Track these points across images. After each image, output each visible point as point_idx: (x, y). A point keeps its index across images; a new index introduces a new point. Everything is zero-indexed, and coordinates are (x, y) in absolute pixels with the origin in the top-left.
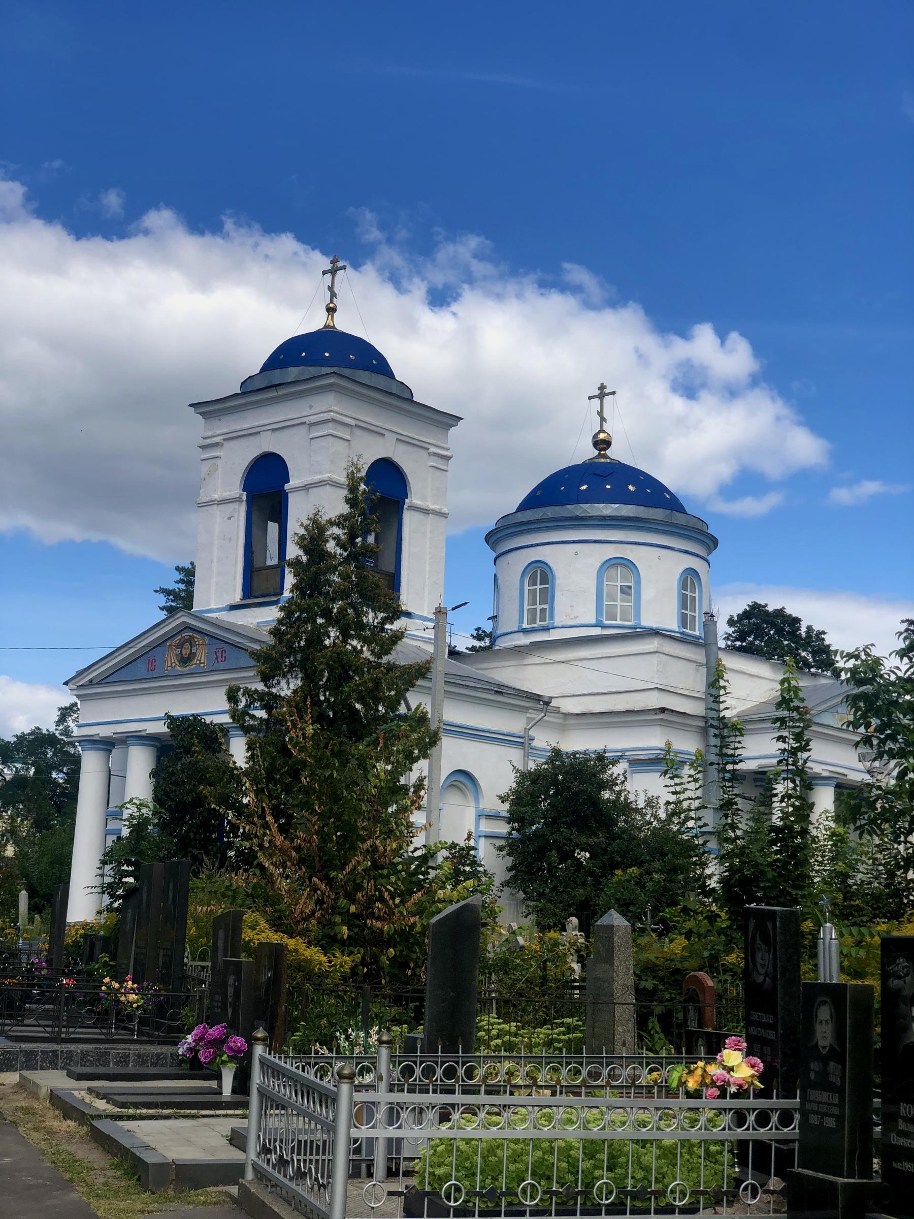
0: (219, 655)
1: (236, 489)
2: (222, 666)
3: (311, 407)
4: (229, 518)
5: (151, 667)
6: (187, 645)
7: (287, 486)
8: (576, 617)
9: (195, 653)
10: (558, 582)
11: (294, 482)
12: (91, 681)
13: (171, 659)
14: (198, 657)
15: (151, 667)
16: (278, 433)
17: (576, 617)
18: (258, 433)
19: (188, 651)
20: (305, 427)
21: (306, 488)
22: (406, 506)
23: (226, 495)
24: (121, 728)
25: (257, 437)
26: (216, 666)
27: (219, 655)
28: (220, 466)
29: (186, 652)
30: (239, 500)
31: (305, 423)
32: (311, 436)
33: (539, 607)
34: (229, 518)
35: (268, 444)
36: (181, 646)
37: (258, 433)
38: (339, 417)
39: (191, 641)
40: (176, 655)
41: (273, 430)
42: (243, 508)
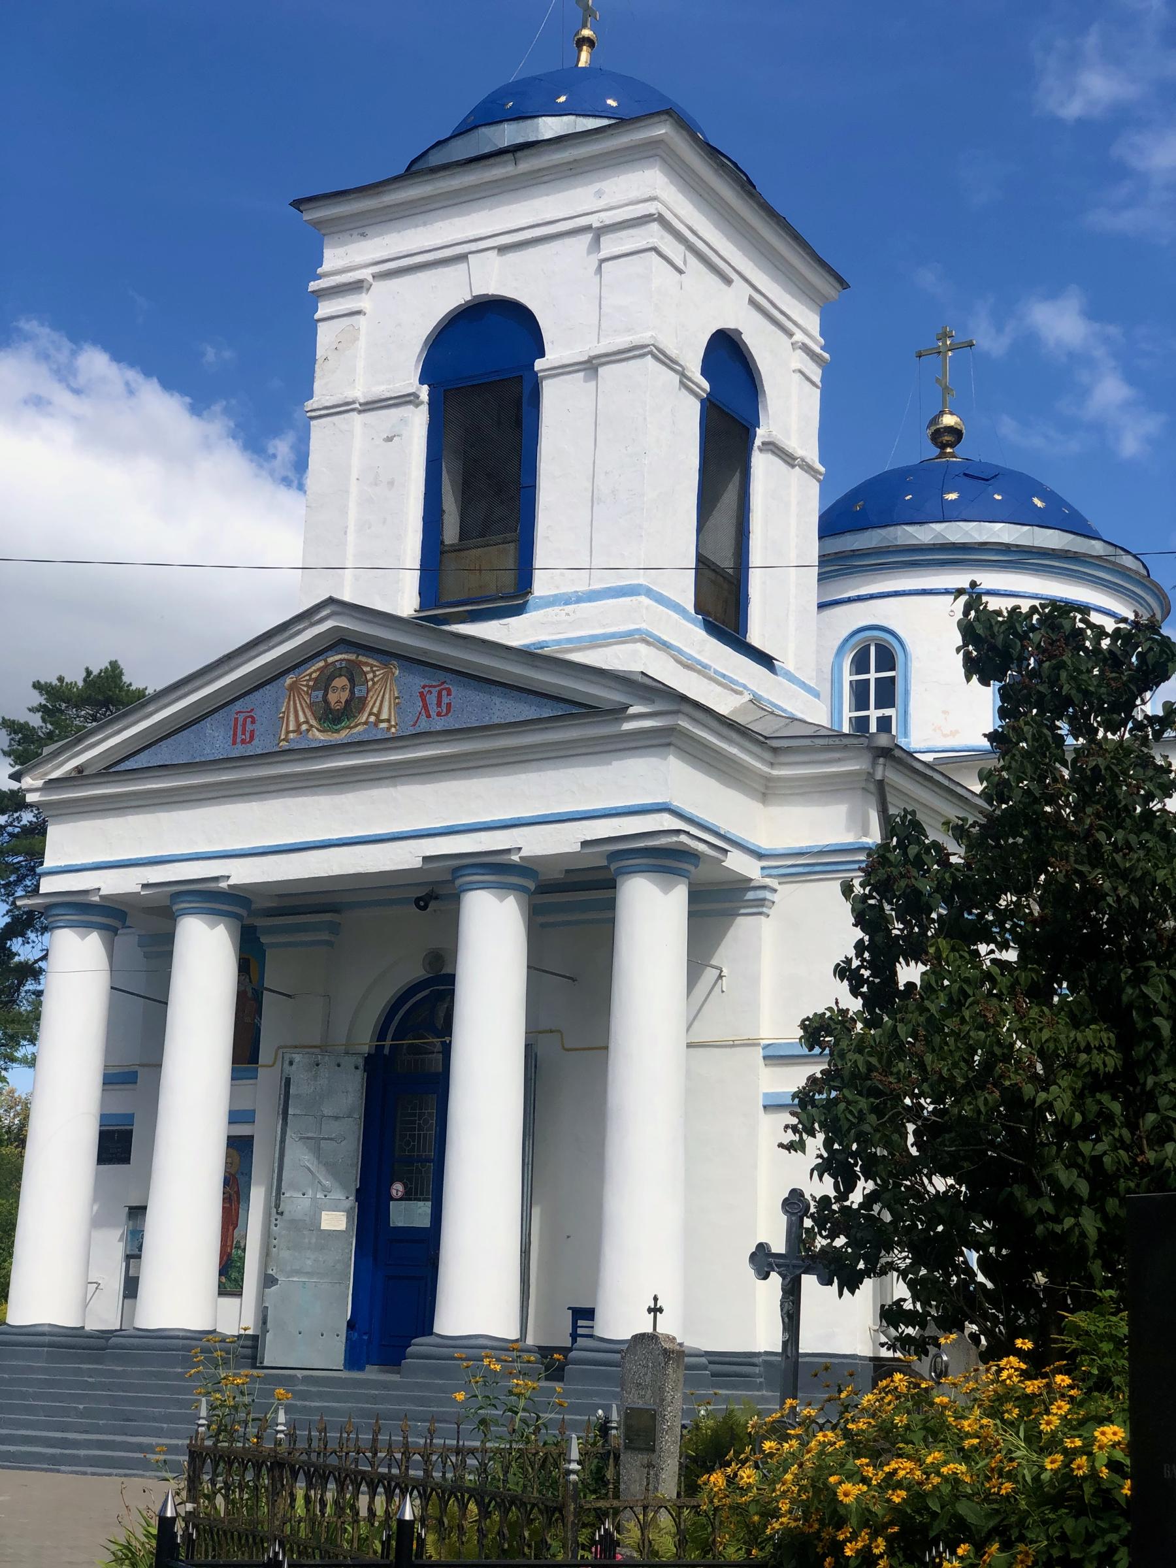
0: (432, 699)
1: (406, 376)
2: (439, 724)
3: (599, 194)
4: (389, 439)
5: (242, 732)
6: (340, 682)
7: (539, 364)
8: (954, 733)
9: (363, 701)
10: (915, 666)
11: (555, 353)
12: (79, 769)
13: (297, 719)
14: (372, 704)
15: (242, 732)
16: (512, 257)
17: (954, 733)
18: (463, 258)
19: (345, 696)
20: (588, 237)
21: (591, 366)
22: (758, 442)
23: (382, 390)
24: (156, 875)
25: (462, 267)
26: (423, 725)
27: (432, 699)
28: (363, 331)
29: (337, 697)
30: (409, 399)
31: (588, 228)
32: (604, 253)
33: (874, 714)
34: (389, 439)
35: (493, 278)
36: (324, 682)
37: (463, 258)
38: (669, 216)
39: (352, 673)
40: (311, 706)
41: (502, 249)
42: (417, 421)
